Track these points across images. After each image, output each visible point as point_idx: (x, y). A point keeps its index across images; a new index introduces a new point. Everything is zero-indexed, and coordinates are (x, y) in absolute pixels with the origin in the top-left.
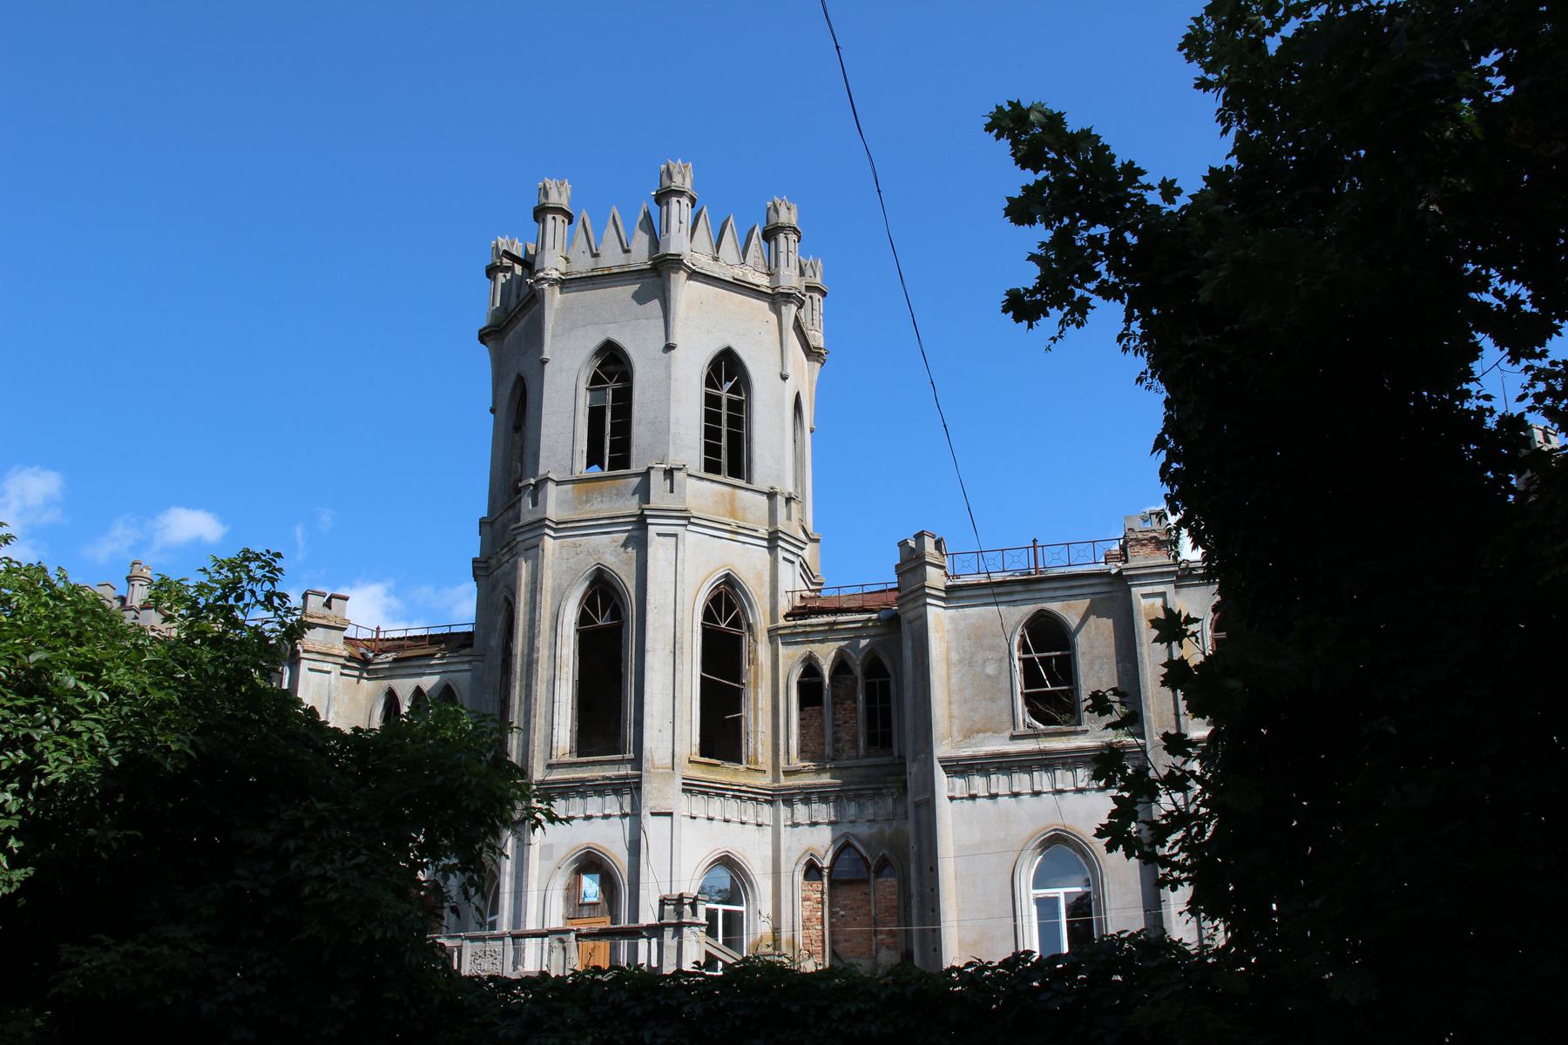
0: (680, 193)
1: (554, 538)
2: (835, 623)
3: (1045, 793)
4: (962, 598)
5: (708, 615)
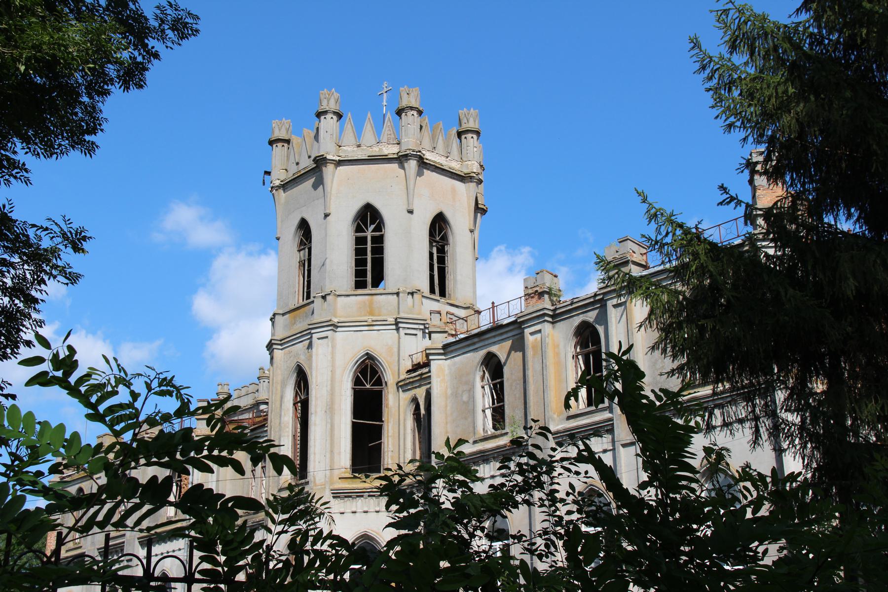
0: (325, 113)
1: (282, 349)
2: (422, 374)
3: (487, 478)
4: (452, 351)
5: (357, 382)
